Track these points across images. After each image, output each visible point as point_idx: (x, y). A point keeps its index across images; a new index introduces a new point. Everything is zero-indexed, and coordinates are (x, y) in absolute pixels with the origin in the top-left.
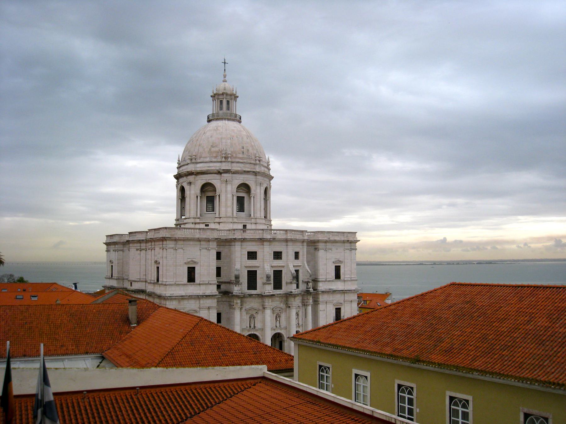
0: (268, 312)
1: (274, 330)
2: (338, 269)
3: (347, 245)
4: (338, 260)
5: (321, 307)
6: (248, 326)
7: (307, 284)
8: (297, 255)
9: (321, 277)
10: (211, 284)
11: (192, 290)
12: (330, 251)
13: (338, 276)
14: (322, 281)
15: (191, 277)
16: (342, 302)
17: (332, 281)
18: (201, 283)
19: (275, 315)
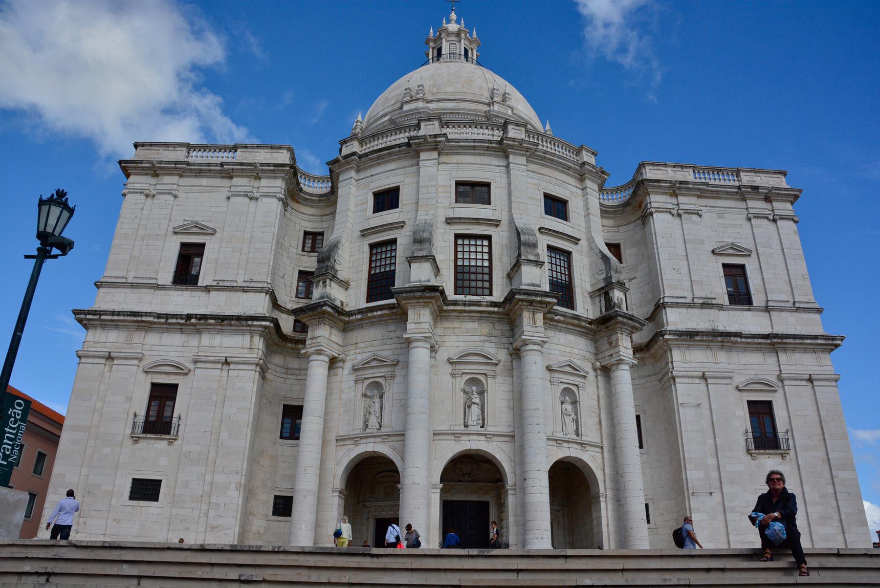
0: (420, 354)
1: (457, 435)
2: (735, 275)
3: (757, 205)
4: (733, 247)
5: (685, 392)
6: (360, 424)
7: (607, 294)
8: (556, 206)
9: (669, 293)
10: (244, 290)
11: (184, 302)
12: (695, 218)
13: (740, 295)
14: (677, 305)
15: (186, 273)
16: (773, 379)
17: (720, 307)
18: (215, 284)
19: (461, 382)
